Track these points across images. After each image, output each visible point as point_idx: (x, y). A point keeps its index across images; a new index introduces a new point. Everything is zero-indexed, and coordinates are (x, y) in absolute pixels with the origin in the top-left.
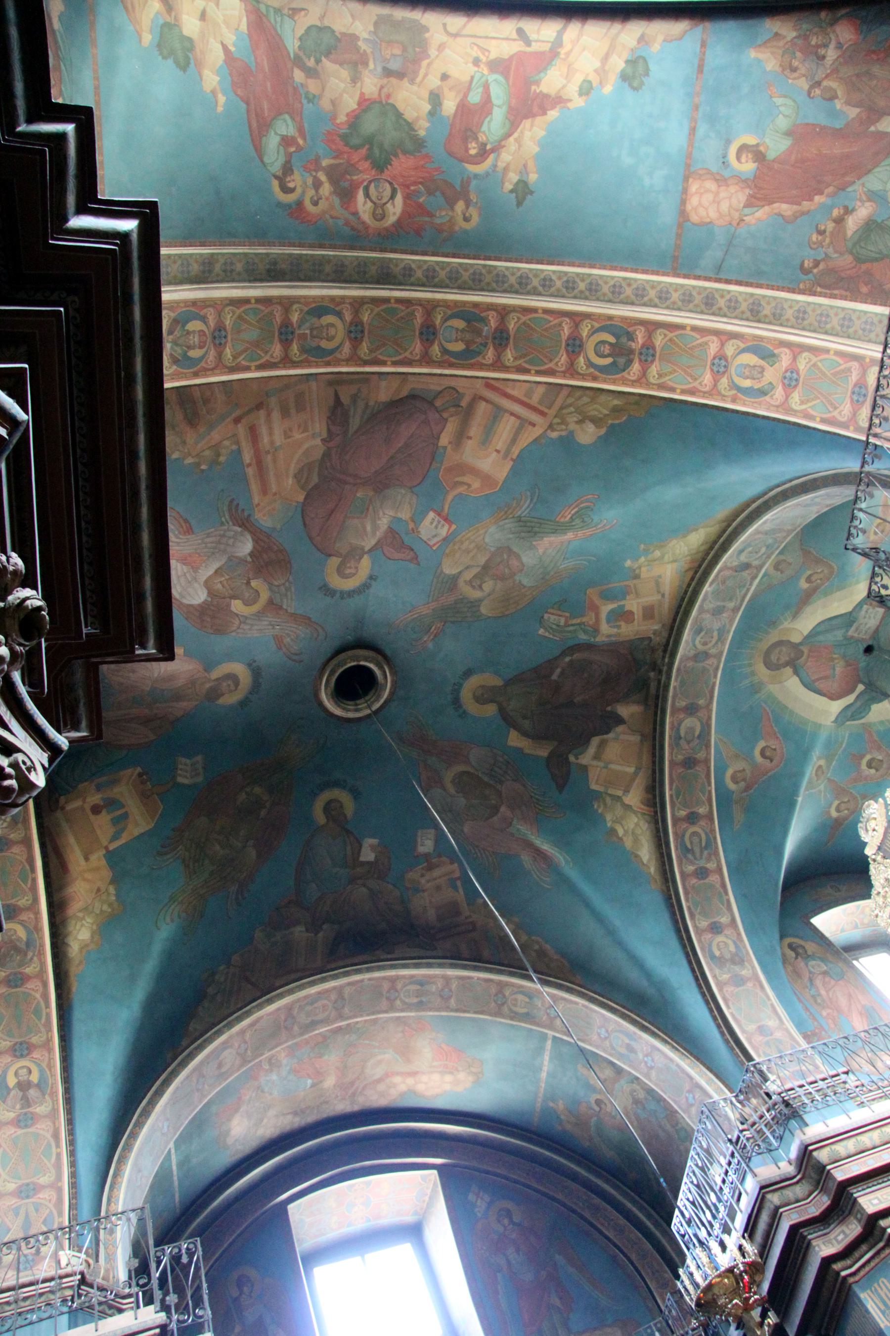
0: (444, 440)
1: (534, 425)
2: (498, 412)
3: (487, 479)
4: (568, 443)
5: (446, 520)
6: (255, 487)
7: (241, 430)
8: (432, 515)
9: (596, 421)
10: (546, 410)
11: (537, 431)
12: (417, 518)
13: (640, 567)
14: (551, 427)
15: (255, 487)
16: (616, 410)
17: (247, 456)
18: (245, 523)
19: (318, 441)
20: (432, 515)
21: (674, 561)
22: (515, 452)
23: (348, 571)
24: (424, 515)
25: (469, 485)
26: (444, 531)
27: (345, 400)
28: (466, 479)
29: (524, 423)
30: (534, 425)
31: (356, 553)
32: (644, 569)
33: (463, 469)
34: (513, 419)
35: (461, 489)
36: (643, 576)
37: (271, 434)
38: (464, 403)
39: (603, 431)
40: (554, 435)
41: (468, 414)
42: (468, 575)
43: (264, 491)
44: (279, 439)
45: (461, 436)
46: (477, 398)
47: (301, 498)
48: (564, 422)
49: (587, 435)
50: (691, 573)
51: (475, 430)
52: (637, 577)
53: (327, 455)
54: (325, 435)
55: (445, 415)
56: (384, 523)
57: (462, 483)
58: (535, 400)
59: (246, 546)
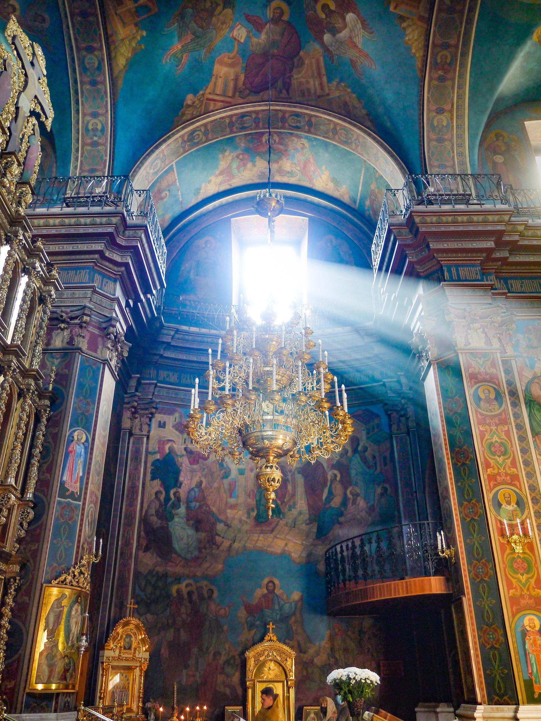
0: (242, 77)
1: (210, 93)
2: (224, 94)
3: (222, 63)
4: (195, 92)
5: (235, 39)
6: (322, 64)
7: (327, 90)
8: (242, 41)
9: (189, 106)
10: (207, 101)
11: (208, 91)
12: (248, 37)
13: (137, 32)
14: (203, 95)
15: (322, 64)
16: (183, 115)
17: (325, 79)
18: (326, 49)
19: (295, 76)
20: (242, 41)
21: (123, 40)
22: (213, 79)
23: (278, 11)
24: (245, 40)
25: (229, 58)
26: (235, 33)
27: (284, 92)
28: (230, 61)
29: (213, 93)
30: (210, 93)
31: (276, 20)
32: (134, 31)
33: (232, 65)
34: (218, 93)
35: (231, 55)
36: (132, 26)
37: (315, 84)
38: (237, 94)
39: (185, 104)
40: (201, 92)
41: (235, 88)
42: (219, 8)
43: (318, 61)
44: (312, 82)
45: (236, 80)
46: (233, 96)
47: (301, 53)
48: (199, 100)
49: (189, 99)
50: (110, 32)
51: (231, 84)
52: (136, 25)
53: (291, 70)
54: (292, 79)
55: (244, 87)
56: (263, 36)
57: (232, 59)
58: (212, 103)
59: (327, 37)
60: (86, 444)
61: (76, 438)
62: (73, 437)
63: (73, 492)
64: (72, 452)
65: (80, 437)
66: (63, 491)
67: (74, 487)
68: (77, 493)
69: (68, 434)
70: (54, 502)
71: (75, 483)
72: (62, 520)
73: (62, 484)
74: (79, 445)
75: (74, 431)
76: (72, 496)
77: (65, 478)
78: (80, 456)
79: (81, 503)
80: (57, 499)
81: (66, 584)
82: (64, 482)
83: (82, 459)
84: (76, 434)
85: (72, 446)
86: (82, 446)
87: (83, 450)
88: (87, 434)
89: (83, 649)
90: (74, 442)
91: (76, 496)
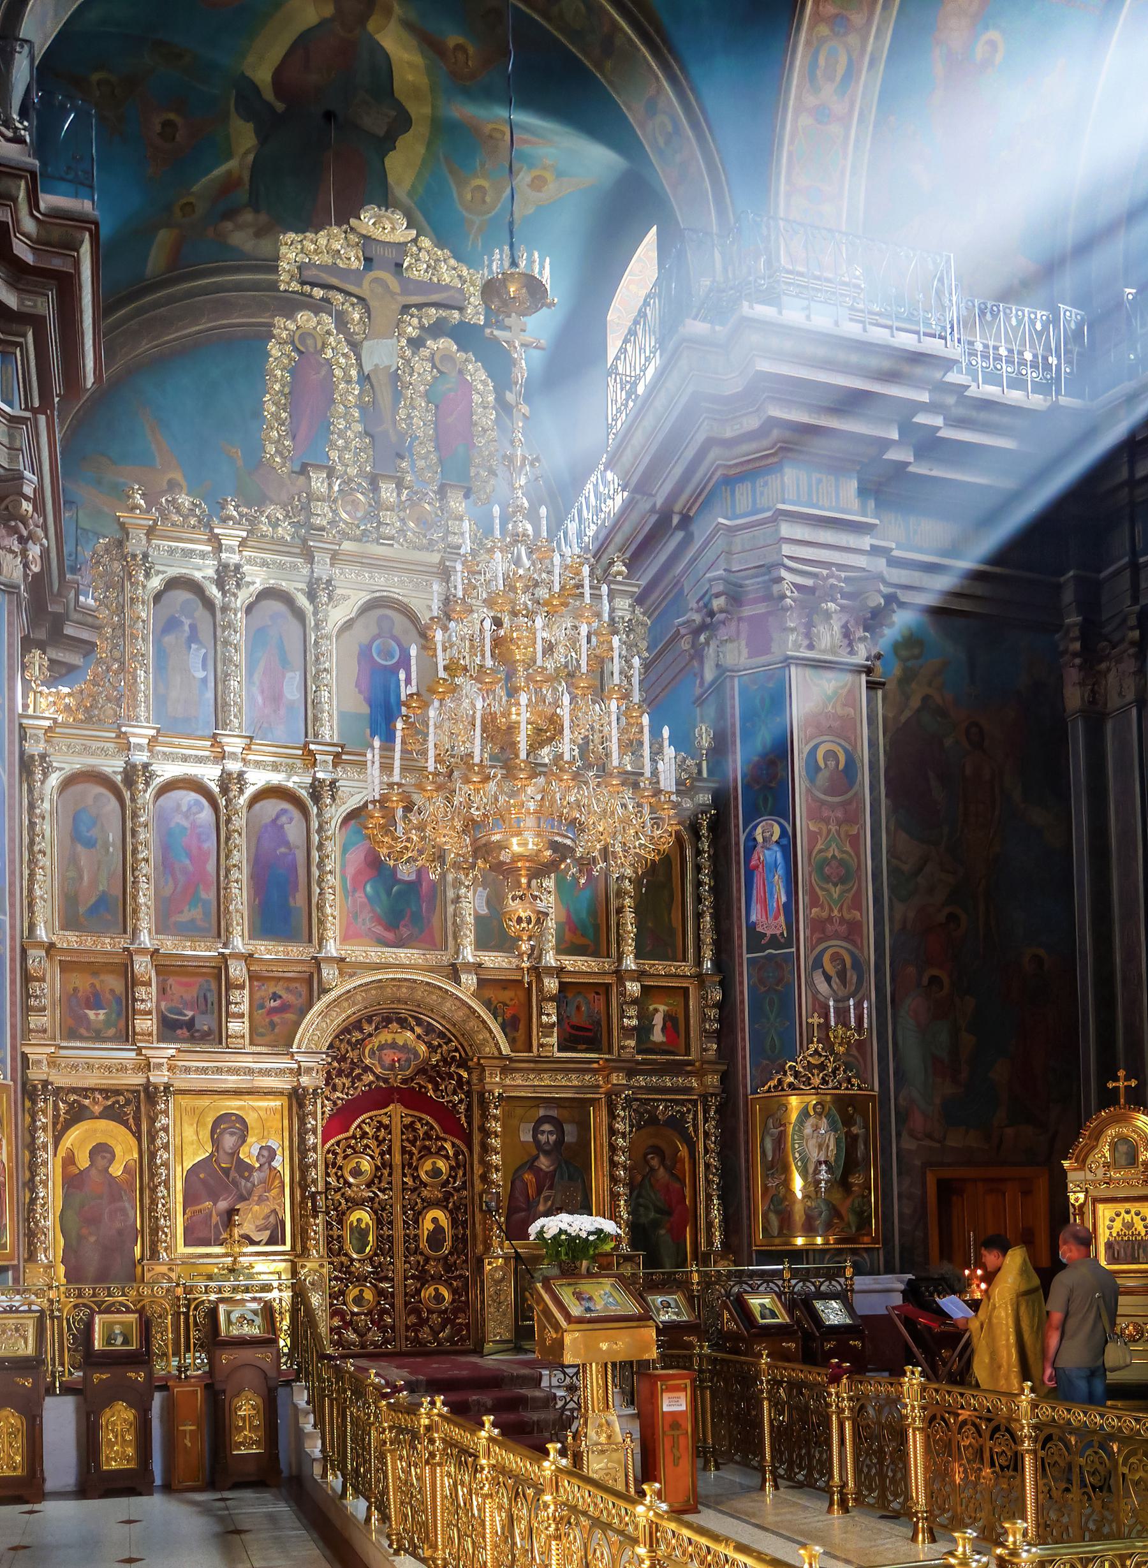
60: (784, 841)
61: (760, 839)
62: (755, 839)
63: (773, 936)
64: (757, 867)
65: (767, 834)
66: (756, 939)
67: (772, 925)
68: (782, 934)
69: (742, 838)
70: (741, 965)
71: (776, 918)
72: (763, 989)
73: (751, 927)
74: (768, 849)
75: (755, 827)
76: (774, 942)
77: (753, 918)
78: (776, 867)
79: (794, 950)
80: (746, 956)
81: (783, 1090)
82: (754, 924)
83: (780, 871)
84: (759, 830)
85: (755, 856)
86: (776, 848)
87: (779, 855)
88: (782, 821)
89: (823, 1184)
90: (758, 848)
91: (782, 940)
